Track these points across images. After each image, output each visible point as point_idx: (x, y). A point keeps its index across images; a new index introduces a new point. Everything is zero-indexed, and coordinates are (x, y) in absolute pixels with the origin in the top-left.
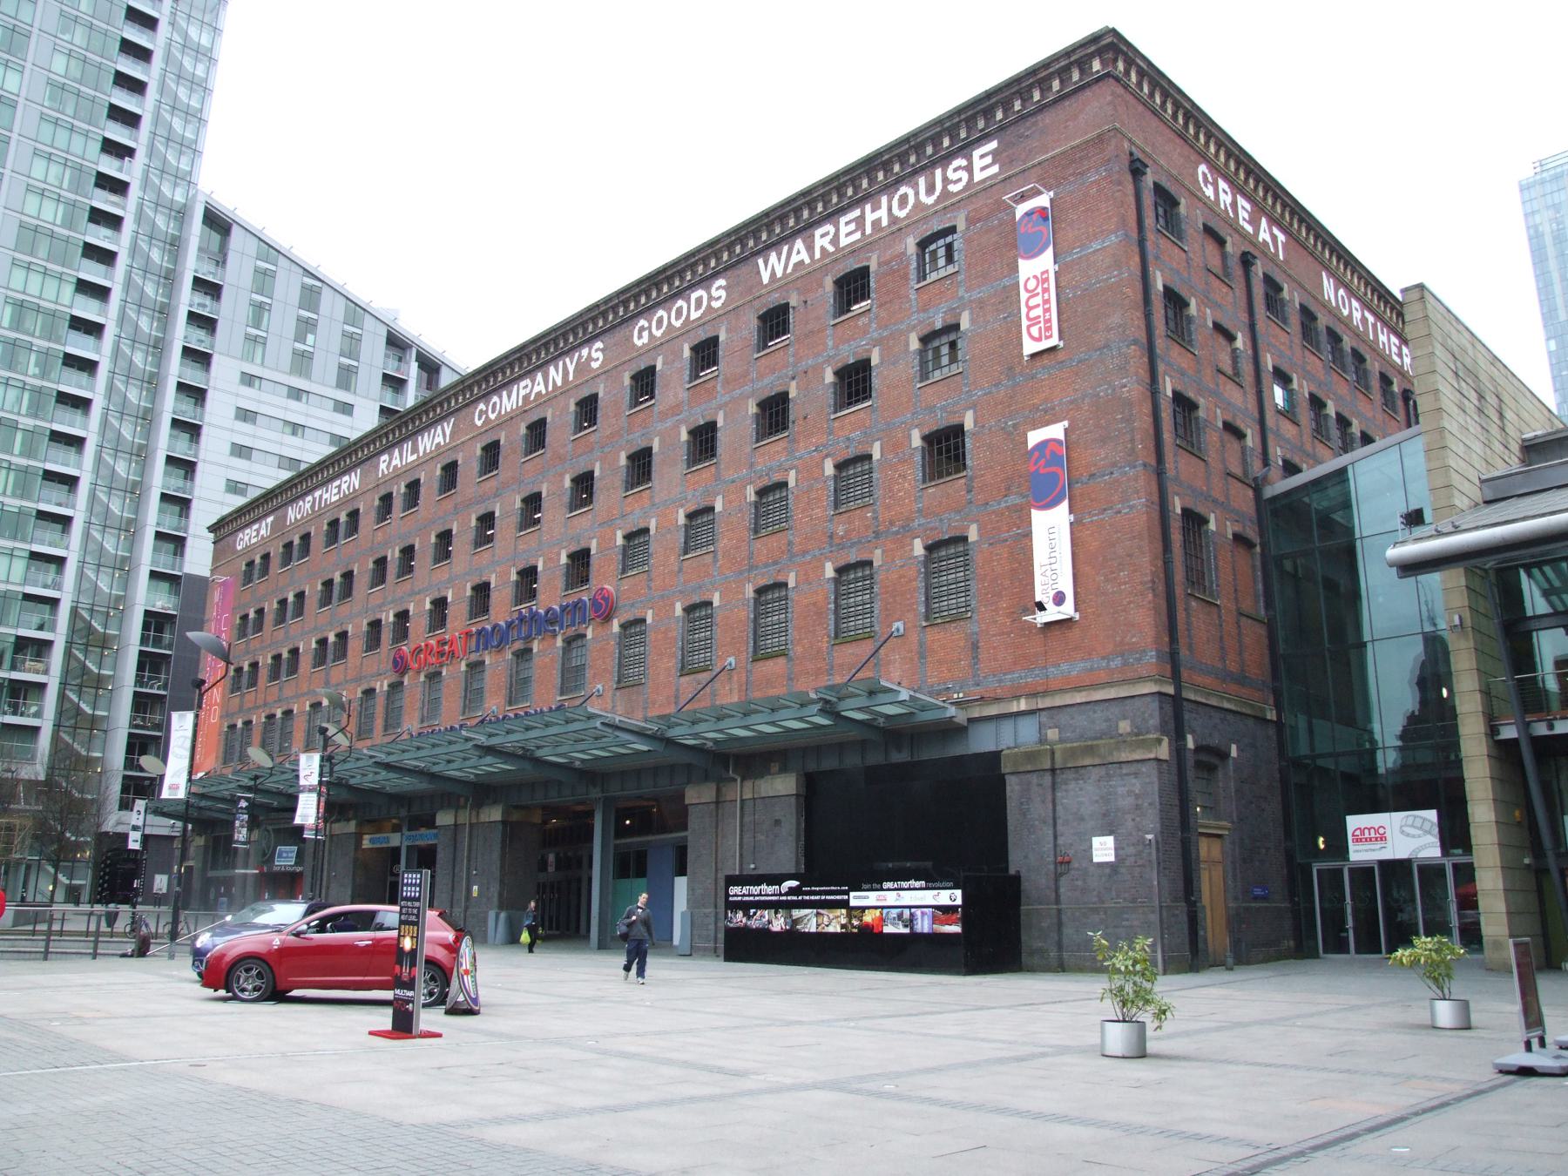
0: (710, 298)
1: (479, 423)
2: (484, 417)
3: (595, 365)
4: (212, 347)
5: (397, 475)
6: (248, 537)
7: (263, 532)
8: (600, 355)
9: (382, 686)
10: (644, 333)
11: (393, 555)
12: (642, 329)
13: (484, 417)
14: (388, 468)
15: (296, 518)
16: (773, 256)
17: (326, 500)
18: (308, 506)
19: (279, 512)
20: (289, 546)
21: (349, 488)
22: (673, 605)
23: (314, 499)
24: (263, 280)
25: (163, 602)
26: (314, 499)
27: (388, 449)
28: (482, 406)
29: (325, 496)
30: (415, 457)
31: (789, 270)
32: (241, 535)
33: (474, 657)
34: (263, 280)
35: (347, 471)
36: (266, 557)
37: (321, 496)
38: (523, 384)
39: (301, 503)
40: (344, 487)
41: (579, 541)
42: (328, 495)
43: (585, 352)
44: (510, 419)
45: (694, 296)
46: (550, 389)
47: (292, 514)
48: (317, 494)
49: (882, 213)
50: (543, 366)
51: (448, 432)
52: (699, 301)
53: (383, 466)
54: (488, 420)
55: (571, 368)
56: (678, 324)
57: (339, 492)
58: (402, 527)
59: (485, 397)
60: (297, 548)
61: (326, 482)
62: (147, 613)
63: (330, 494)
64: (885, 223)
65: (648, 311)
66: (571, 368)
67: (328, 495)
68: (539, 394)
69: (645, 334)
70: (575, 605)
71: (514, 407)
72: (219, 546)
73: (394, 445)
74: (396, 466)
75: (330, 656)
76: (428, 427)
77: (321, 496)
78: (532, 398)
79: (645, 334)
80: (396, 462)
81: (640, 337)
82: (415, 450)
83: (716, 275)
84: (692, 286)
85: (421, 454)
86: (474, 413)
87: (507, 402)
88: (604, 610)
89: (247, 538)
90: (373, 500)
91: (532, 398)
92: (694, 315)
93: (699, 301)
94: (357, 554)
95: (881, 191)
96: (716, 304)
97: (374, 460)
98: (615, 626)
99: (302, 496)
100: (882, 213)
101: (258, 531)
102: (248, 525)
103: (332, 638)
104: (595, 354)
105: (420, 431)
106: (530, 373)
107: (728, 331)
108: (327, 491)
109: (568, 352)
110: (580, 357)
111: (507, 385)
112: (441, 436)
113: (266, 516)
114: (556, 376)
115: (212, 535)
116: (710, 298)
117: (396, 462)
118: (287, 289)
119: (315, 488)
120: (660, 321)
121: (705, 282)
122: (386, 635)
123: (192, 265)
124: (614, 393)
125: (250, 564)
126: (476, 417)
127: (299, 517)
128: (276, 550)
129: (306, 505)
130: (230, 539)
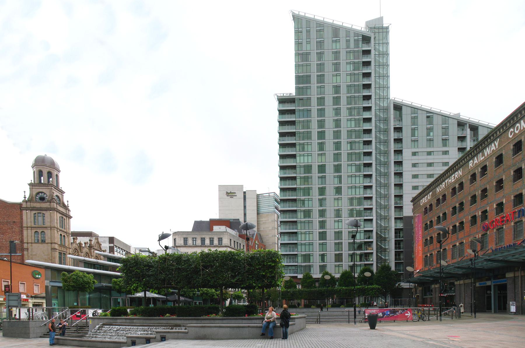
1: (510, 137)
2: (513, 134)
4: (402, 147)
5: (477, 166)
6: (424, 201)
7: (429, 198)
9: (478, 236)
11: (478, 193)
13: (513, 134)
14: (473, 165)
15: (440, 190)
17: (450, 182)
18: (443, 186)
19: (434, 190)
20: (438, 200)
21: (458, 176)
23: (446, 183)
24: (414, 120)
25: (400, 225)
26: (446, 183)
27: (472, 158)
29: (449, 181)
30: (483, 157)
32: (421, 201)
33: (517, 220)
34: (414, 120)
35: (457, 170)
36: (431, 205)
39: (441, 185)
40: (456, 176)
42: (450, 180)
47: (438, 190)
48: (446, 181)
51: (497, 144)
53: (470, 165)
54: (515, 134)
57: (455, 178)
58: (480, 184)
60: (442, 200)
61: (449, 177)
62: (395, 229)
63: (452, 180)
67: (450, 180)
72: (415, 205)
73: (474, 157)
75: (458, 230)
76: (488, 146)
82: (483, 155)
85: (486, 156)
86: (508, 134)
89: (423, 201)
90: (468, 177)
94: (464, 196)
97: (467, 164)
99: (441, 183)
101: (427, 198)
102: (424, 197)
103: (458, 224)
105: (485, 148)
108: (450, 179)
113: (429, 193)
115: (412, 203)
117: (476, 161)
118: (422, 119)
119: (445, 180)
122: (479, 220)
123: (392, 124)
125: (426, 208)
127: (441, 190)
128: (434, 202)
129: (443, 185)
130: (418, 203)
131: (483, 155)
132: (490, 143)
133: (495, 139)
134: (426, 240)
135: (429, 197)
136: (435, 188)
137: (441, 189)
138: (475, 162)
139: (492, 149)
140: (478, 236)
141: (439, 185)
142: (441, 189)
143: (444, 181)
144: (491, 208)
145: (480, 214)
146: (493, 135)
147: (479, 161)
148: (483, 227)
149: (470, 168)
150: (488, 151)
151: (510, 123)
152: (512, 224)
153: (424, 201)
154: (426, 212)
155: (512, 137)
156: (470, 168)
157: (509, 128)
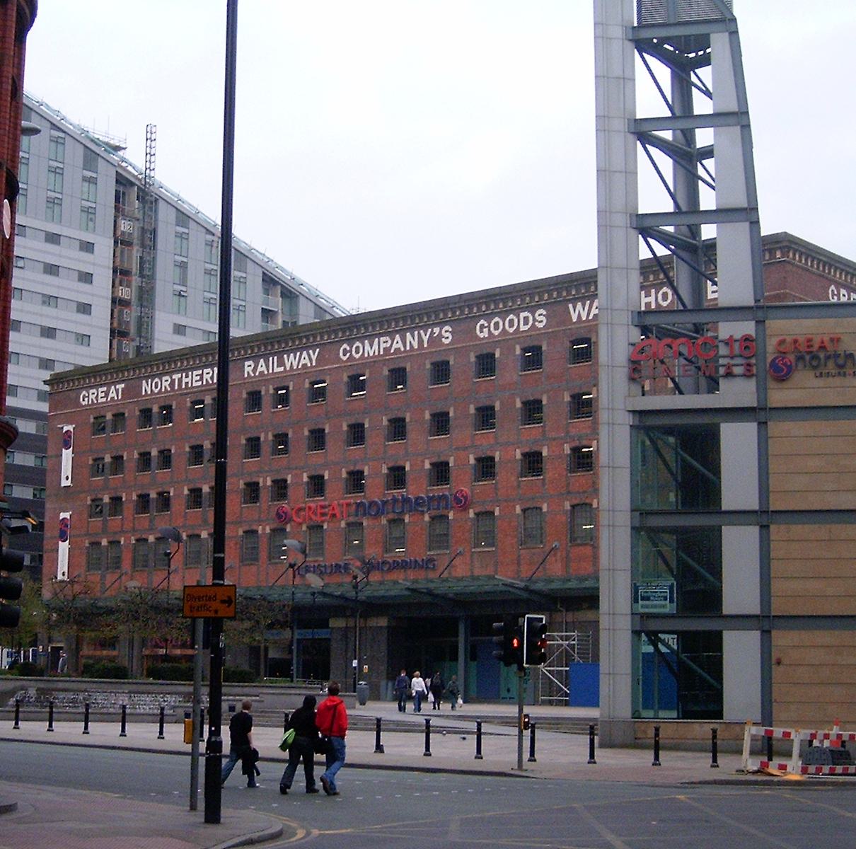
0: (534, 320)
2: (348, 354)
3: (446, 342)
6: (92, 396)
7: (112, 394)
8: (447, 334)
9: (264, 529)
10: (484, 330)
11: (267, 438)
12: (482, 327)
13: (348, 354)
14: (254, 370)
16: (579, 305)
22: (514, 507)
23: (173, 381)
26: (173, 381)
27: (256, 359)
28: (345, 346)
29: (185, 380)
30: (282, 369)
31: (590, 318)
33: (352, 519)
36: (119, 416)
37: (180, 380)
38: (383, 339)
41: (439, 456)
42: (189, 380)
43: (437, 330)
44: (373, 363)
45: (523, 315)
46: (408, 348)
47: (146, 387)
48: (176, 377)
49: (652, 299)
50: (402, 333)
51: (314, 358)
52: (526, 319)
55: (425, 339)
56: (511, 330)
57: (201, 379)
59: (350, 342)
64: (653, 306)
65: (489, 317)
66: (425, 339)
67: (189, 380)
68: (397, 350)
69: (486, 330)
70: (440, 497)
71: (376, 354)
73: (260, 357)
74: (261, 373)
76: (294, 351)
77: (180, 380)
78: (392, 351)
79: (486, 330)
80: (262, 367)
81: (481, 332)
82: (281, 363)
83: (540, 306)
84: (523, 310)
85: (288, 369)
87: (372, 349)
88: (462, 503)
90: (241, 393)
91: (392, 351)
92: (523, 328)
93: (526, 320)
95: (653, 286)
96: (540, 326)
98: (471, 514)
99: (160, 376)
100: (652, 299)
101: (107, 395)
102: (96, 387)
104: (446, 334)
106: (391, 335)
107: (548, 345)
109: (425, 327)
110: (432, 333)
111: (371, 338)
112: (307, 358)
113: (115, 383)
114: (412, 340)
116: (534, 320)
117: (262, 367)
120: (497, 325)
121: (532, 310)
122: (265, 496)
124: (464, 365)
126: (341, 354)
127: (156, 391)
128: (133, 413)
129: (165, 382)
130: (73, 395)
131: (281, 363)
132: (301, 349)
133: (313, 347)
134: (96, 501)
135: (116, 392)
136: (140, 378)
137: (156, 387)
138: (259, 369)
139: (303, 362)
140: (264, 529)
141: (153, 377)
142: (156, 387)
143: (170, 373)
144: (298, 480)
145: (269, 483)
146: (307, 337)
147: (271, 371)
148: (278, 514)
149: (246, 376)
150: (291, 361)
151: (344, 332)
152: (343, 524)
153: (92, 396)
154: (99, 427)
155: (347, 361)
156: (246, 376)
157: (341, 342)
